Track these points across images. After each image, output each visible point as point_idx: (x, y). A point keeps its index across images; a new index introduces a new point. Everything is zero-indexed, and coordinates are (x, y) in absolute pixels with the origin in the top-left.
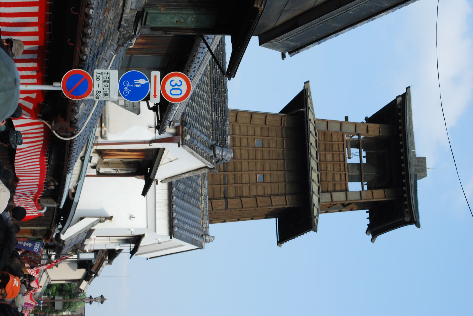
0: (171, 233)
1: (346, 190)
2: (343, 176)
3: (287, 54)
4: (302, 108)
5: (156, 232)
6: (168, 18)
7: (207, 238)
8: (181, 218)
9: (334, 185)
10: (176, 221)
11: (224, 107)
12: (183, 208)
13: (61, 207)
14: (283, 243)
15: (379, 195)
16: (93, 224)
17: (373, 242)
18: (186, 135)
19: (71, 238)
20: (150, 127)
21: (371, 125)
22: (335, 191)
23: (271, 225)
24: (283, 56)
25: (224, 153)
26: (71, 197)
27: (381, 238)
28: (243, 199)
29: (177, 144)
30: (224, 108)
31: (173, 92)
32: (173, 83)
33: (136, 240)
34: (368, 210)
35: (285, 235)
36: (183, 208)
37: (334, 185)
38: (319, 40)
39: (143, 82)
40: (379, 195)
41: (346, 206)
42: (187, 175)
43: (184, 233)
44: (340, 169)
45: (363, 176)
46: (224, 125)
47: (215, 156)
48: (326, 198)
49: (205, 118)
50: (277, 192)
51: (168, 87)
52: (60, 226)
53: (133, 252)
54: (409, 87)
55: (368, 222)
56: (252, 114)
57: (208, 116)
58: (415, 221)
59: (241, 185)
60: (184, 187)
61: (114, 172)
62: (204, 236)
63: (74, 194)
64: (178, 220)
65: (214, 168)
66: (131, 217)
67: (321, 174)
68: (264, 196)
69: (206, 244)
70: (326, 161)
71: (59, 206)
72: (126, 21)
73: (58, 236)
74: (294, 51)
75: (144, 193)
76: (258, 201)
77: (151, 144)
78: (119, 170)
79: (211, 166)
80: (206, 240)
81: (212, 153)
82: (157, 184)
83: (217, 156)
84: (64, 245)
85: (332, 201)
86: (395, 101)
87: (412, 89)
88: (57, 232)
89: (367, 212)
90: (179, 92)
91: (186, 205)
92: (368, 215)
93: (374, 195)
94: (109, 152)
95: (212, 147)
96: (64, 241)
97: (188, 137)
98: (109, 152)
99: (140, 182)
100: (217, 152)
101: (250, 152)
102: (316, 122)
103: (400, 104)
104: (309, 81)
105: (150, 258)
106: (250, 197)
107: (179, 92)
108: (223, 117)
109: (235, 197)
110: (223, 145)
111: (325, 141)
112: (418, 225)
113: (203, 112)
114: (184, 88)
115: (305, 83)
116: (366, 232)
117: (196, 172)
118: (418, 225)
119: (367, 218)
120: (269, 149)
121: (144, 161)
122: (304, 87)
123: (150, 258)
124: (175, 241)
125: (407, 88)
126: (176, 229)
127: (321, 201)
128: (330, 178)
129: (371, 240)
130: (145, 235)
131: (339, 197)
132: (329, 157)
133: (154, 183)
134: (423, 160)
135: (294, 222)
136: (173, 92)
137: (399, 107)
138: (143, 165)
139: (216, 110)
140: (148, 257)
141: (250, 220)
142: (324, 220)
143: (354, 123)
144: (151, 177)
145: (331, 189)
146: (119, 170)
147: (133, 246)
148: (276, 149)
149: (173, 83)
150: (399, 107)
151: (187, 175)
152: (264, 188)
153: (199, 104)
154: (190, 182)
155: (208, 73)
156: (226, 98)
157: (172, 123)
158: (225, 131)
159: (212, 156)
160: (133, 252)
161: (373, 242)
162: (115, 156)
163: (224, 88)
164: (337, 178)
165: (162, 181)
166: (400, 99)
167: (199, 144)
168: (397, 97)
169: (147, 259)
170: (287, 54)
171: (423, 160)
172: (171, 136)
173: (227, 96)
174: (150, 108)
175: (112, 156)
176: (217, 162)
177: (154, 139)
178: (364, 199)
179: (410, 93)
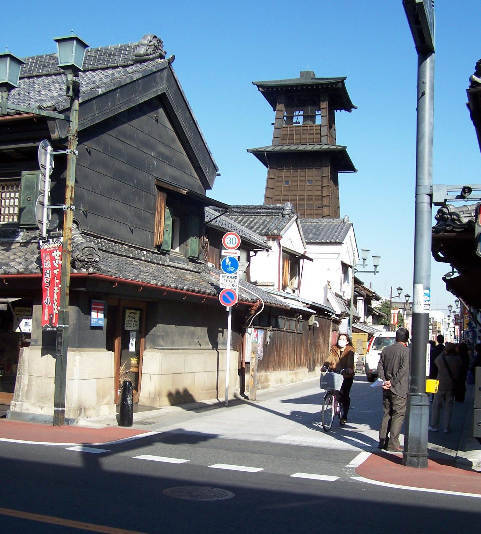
0: (340, 243)
1: (320, 126)
3: (217, 173)
6: (193, 244)
9: (317, 134)
13: (315, 312)
15: (324, 105)
23: (342, 176)
24: (219, 175)
26: (308, 306)
27: (353, 103)
31: (234, 243)
32: (229, 243)
33: (345, 267)
35: (349, 167)
37: (317, 134)
38: (209, 153)
39: (228, 261)
40: (324, 105)
42: (302, 233)
46: (269, 208)
48: (324, 140)
49: (264, 220)
51: (231, 246)
52: (331, 314)
55: (343, 111)
57: (264, 218)
58: (342, 81)
63: (307, 304)
71: (314, 314)
72: (195, 268)
73: (337, 315)
74: (215, 168)
79: (295, 217)
84: (344, 312)
87: (256, 80)
88: (334, 316)
90: (234, 239)
91: (323, 233)
92: (339, 111)
93: (324, 107)
97: (275, 231)
100: (287, 213)
101: (292, 189)
103: (263, 89)
107: (234, 239)
110: (282, 209)
113: (261, 221)
114: (232, 236)
121: (290, 260)
124: (346, 240)
128: (312, 137)
132: (298, 137)
133: (306, 255)
135: (340, 161)
136: (234, 243)
138: (293, 261)
139: (259, 213)
142: (340, 142)
149: (229, 243)
151: (302, 233)
152: (317, 181)
153: (255, 224)
156: (252, 206)
166: (260, 89)
170: (217, 173)
171: (303, 74)
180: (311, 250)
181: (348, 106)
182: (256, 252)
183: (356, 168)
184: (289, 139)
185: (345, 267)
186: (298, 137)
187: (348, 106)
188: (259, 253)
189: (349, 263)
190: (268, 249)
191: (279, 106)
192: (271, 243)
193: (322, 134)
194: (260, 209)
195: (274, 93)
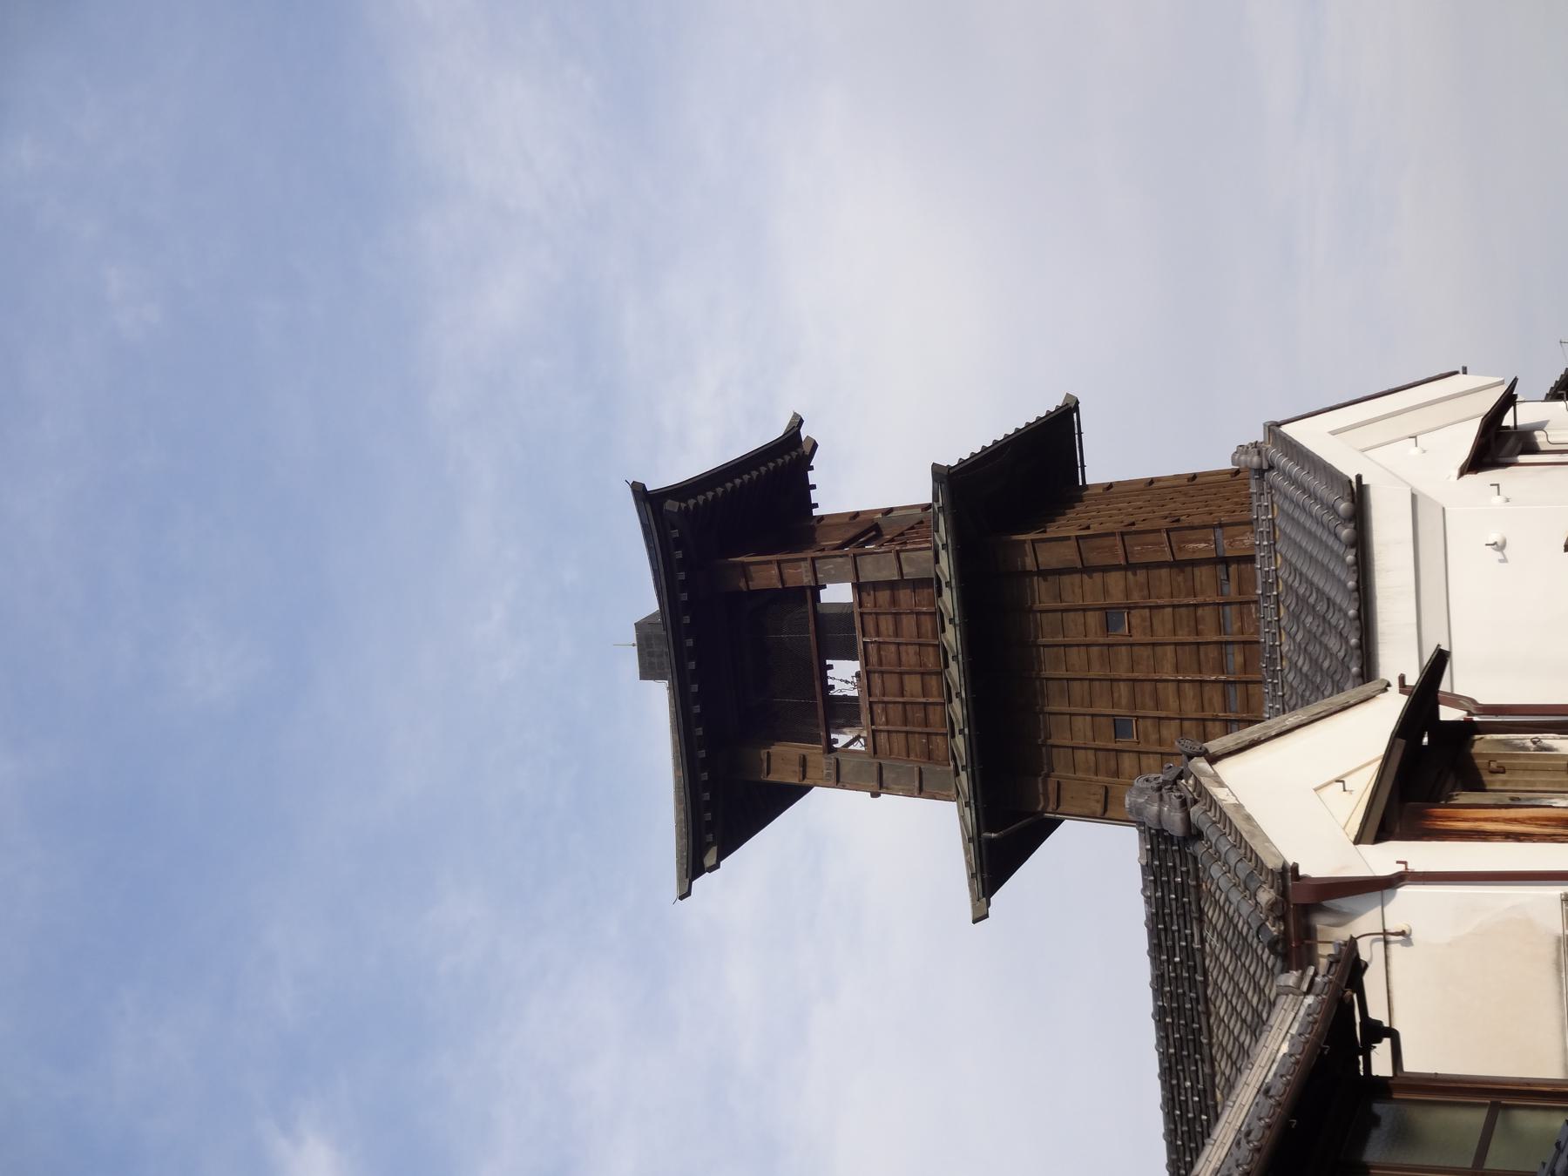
0: (1358, 494)
1: (858, 588)
2: (870, 626)
4: (990, 840)
5: (1414, 497)
7: (1256, 459)
8: (1331, 541)
9: (894, 601)
10: (1346, 532)
11: (1162, 962)
12: (1329, 574)
14: (1058, 409)
15: (765, 573)
17: (796, 415)
18: (1272, 906)
20: (1403, 933)
21: (795, 780)
22: (892, 585)
25: (1155, 808)
27: (775, 431)
29: (1301, 873)
30: (1164, 957)
33: (1497, 445)
34: (815, 512)
36: (1329, 574)
37: (894, 601)
40: (765, 573)
41: (867, 530)
42: (1291, 720)
43: (1321, 489)
44: (879, 650)
45: (812, 627)
47: (1184, 803)
48: (916, 563)
50: (1066, 579)
53: (1508, 400)
54: (682, 898)
55: (813, 477)
59: (1176, 601)
60: (1325, 639)
62: (1265, 466)
64: (1336, 536)
65: (1190, 757)
66: (1500, 547)
67: (936, 636)
69: (1261, 439)
70: (922, 674)
75: (1439, 662)
76: (1120, 551)
77: (1401, 868)
78: (1530, 744)
79: (1202, 764)
80: (1259, 453)
81: (1195, 811)
82: (1402, 679)
83: (1177, 802)
85: (898, 553)
86: (722, 855)
87: (673, 888)
89: (816, 506)
91: (1318, 580)
92: (815, 496)
93: (775, 572)
94: (1560, 831)
95: (1193, 834)
97: (1266, 896)
98: (1560, 831)
99: (1462, 681)
102: (953, 791)
103: (709, 846)
104: (975, 921)
106: (1147, 566)
108: (1165, 929)
109: (1194, 563)
111: (928, 734)
112: (639, 491)
115: (986, 916)
116: (815, 446)
117: (1255, 736)
118: (639, 491)
119: (814, 487)
120: (1091, 711)
122: (988, 904)
125: (688, 894)
126: (1343, 506)
127: (931, 553)
128: (908, 623)
129: (801, 421)
130: (1456, 472)
131: (879, 567)
133: (1413, 679)
134: (648, 671)
135: (1024, 477)
137: (710, 838)
139: (1189, 952)
140: (1460, 377)
141: (1159, 479)
142: (920, 491)
143: (844, 787)
144: (1402, 742)
145: (905, 595)
146: (1530, 744)
147: (1508, 420)
148: (1073, 709)
150: (710, 838)
152: (1106, 592)
154: (1310, 648)
155: (1223, 1065)
156: (1158, 992)
157: (1305, 987)
158: (1155, 882)
159: (1195, 802)
160: (1508, 400)
161: (796, 415)
162: (1537, 819)
163: (1167, 1024)
164: (886, 624)
165: (1385, 690)
166: (710, 860)
167: (1233, 860)
168: (716, 866)
172: (1326, 903)
173: (1156, 999)
174: (1393, 1034)
175: (1549, 819)
176: (1180, 777)
177: (1386, 892)
178: (804, 559)
179: (680, 880)
180: (1399, 660)
181: (788, 458)
182: (1376, 1031)
183: (1052, 403)
185: (1497, 445)
187: (788, 458)
188: (1377, 1012)
189: (1471, 430)
190: (1351, 968)
191: (785, 774)
192: (1330, 935)
194: (1171, 952)
195: (724, 806)
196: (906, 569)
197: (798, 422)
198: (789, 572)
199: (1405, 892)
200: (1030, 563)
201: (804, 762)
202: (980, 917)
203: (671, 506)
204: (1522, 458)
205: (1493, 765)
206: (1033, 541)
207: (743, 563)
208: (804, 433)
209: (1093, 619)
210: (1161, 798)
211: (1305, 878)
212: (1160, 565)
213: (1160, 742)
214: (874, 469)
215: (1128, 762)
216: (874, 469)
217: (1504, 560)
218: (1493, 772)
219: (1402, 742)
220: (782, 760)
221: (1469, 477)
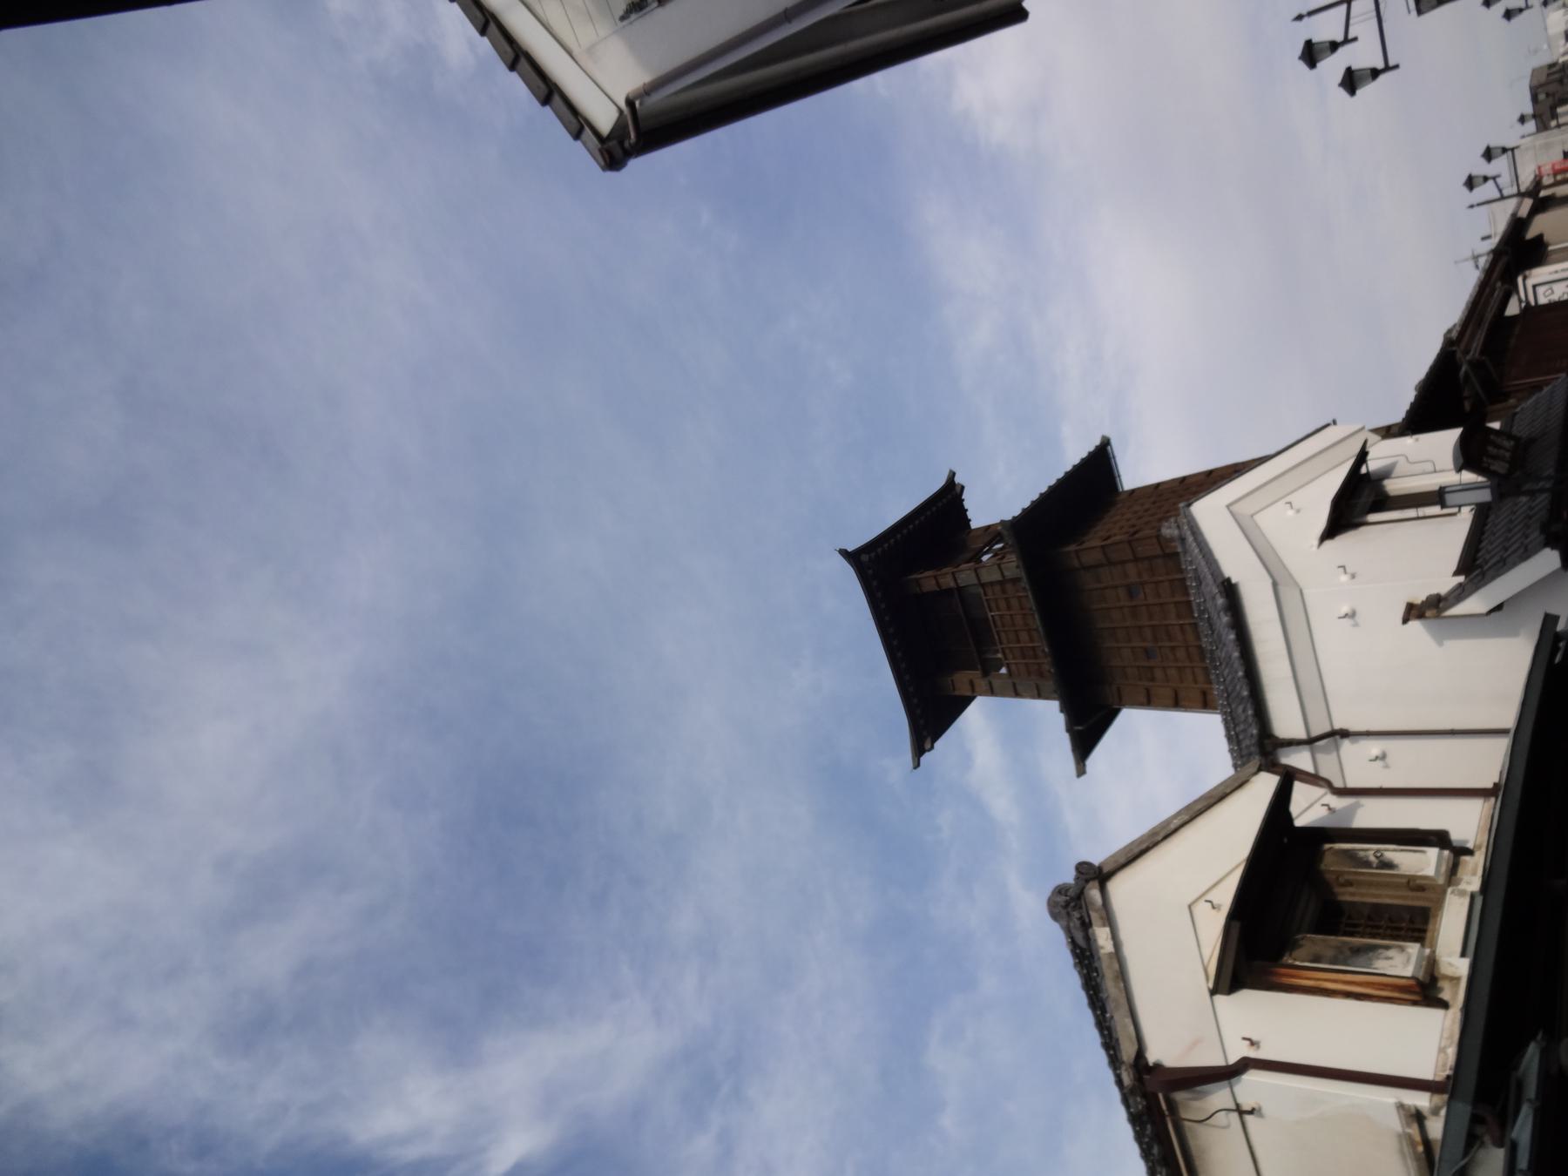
2: (993, 605)
9: (1004, 591)
16: (1460, 594)
19: (1526, 554)
22: (1002, 583)
28: (1159, 552)
37: (1004, 591)
40: (928, 581)
56: (1177, 703)
58: (852, 557)
61: (1394, 854)
66: (1352, 615)
68: (1123, 562)
92: (970, 515)
96: (1546, 545)
105: (1327, 425)
106: (1148, 558)
123: (1327, 425)
128: (1014, 602)
130: (1316, 542)
132: (1024, 636)
145: (1009, 587)
146: (1372, 858)
147: (1363, 470)
160: (1362, 456)
164: (1003, 604)
166: (928, 746)
169: (1335, 422)
183: (1097, 442)
184: (1036, 657)
186: (1024, 636)
193: (999, 578)
195: (930, 715)
196: (1006, 573)
197: (952, 475)
198: (941, 581)
199: (1252, 1077)
200: (1076, 563)
201: (972, 684)
202: (1081, 771)
203: (865, 558)
204: (1372, 517)
205: (1341, 880)
206: (1077, 552)
207: (917, 580)
208: (957, 480)
209: (1122, 592)
210: (1068, 914)
211: (1158, 1067)
212: (1156, 557)
213: (1176, 660)
214: (994, 501)
215: (1159, 674)
216: (994, 501)
217: (1356, 625)
218: (1343, 885)
219: (1236, 925)
220: (960, 681)
221: (1328, 544)
